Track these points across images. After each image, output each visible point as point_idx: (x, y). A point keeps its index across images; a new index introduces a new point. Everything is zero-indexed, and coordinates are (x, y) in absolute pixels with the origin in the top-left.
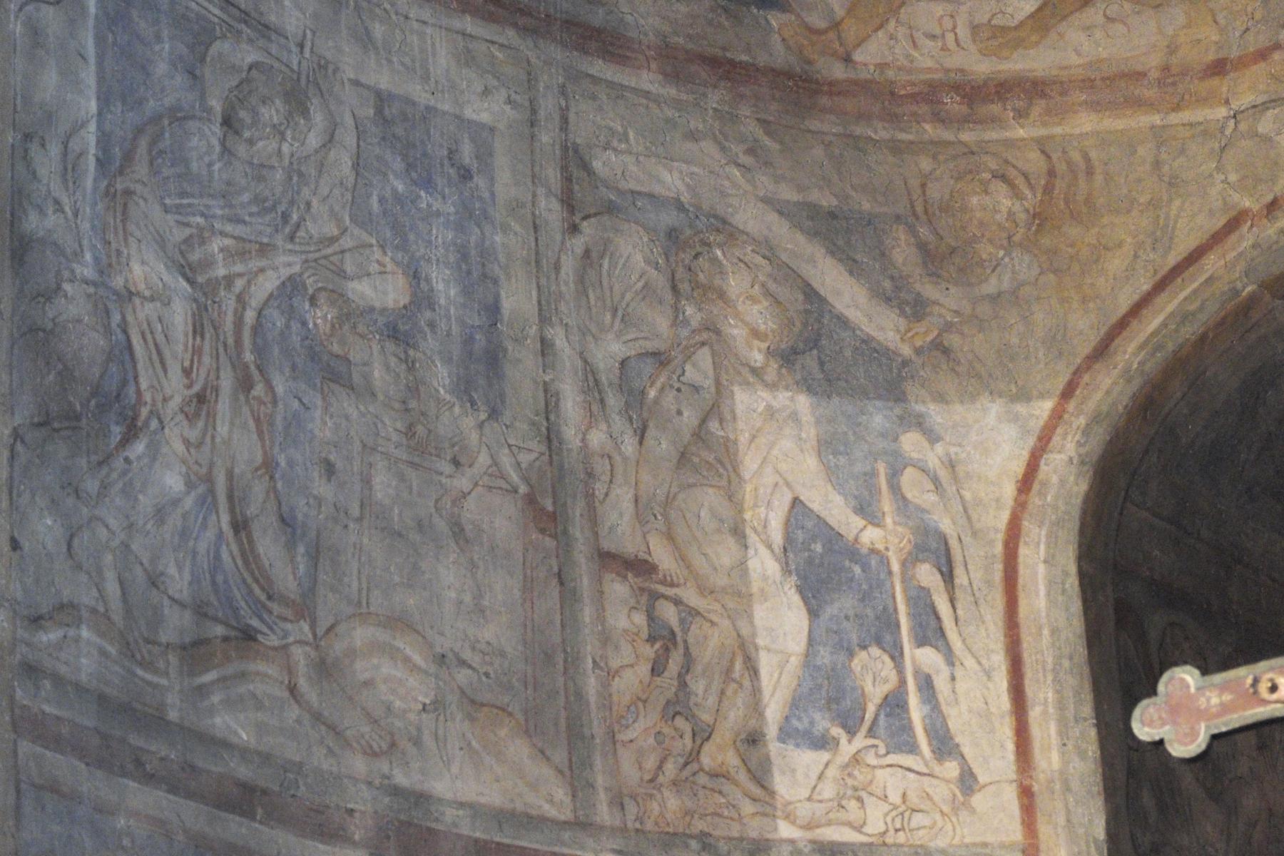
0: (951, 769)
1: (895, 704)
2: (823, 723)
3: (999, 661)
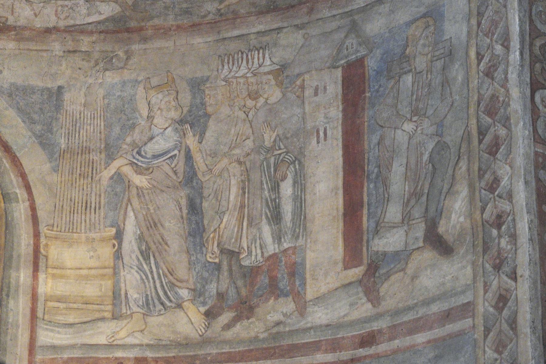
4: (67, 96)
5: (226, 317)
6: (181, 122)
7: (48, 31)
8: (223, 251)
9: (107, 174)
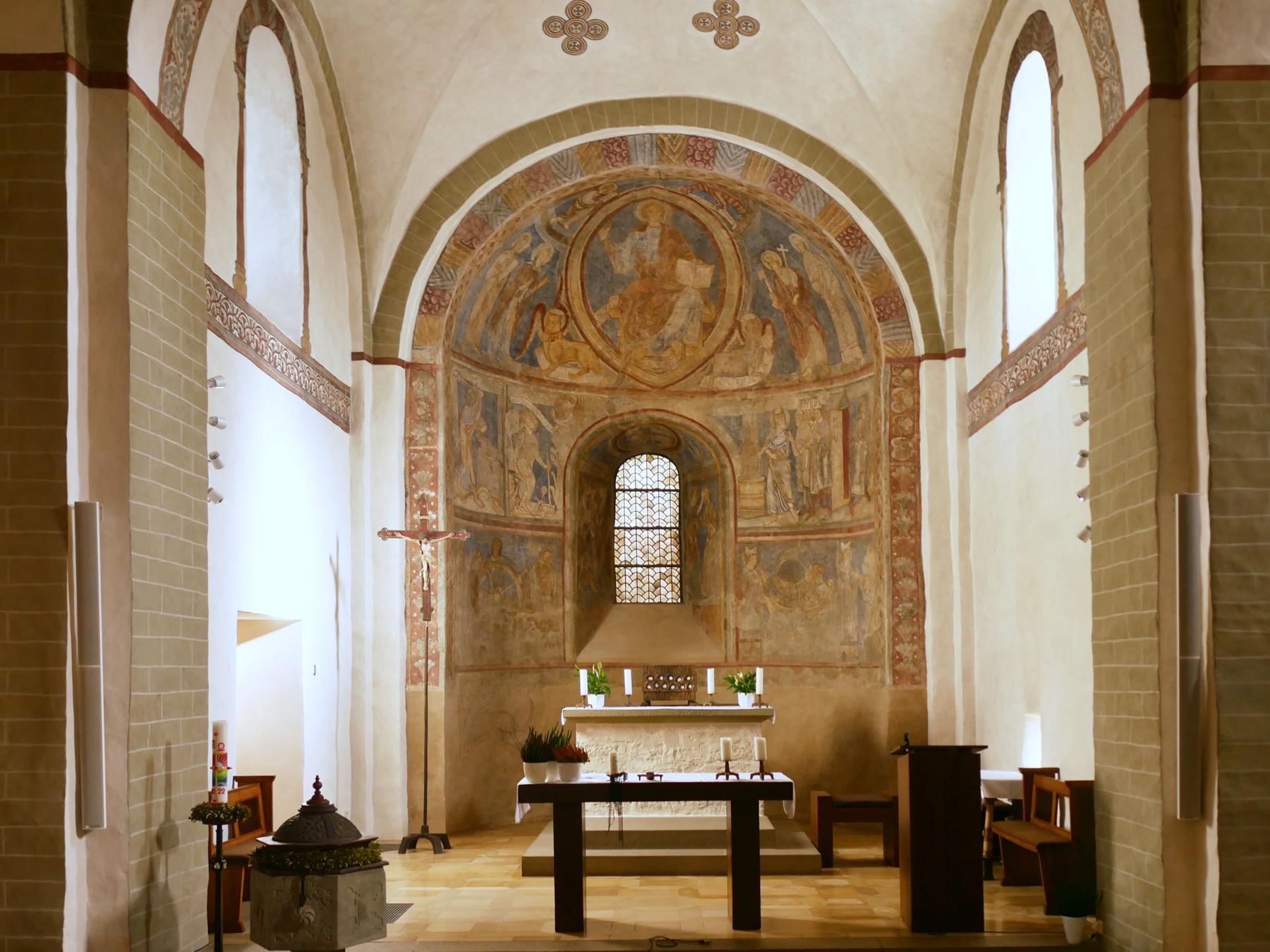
0: (554, 507)
1: (547, 495)
2: (536, 498)
3: (562, 489)
4: (744, 420)
5: (805, 517)
6: (787, 430)
7: (734, 391)
8: (804, 487)
9: (760, 454)
